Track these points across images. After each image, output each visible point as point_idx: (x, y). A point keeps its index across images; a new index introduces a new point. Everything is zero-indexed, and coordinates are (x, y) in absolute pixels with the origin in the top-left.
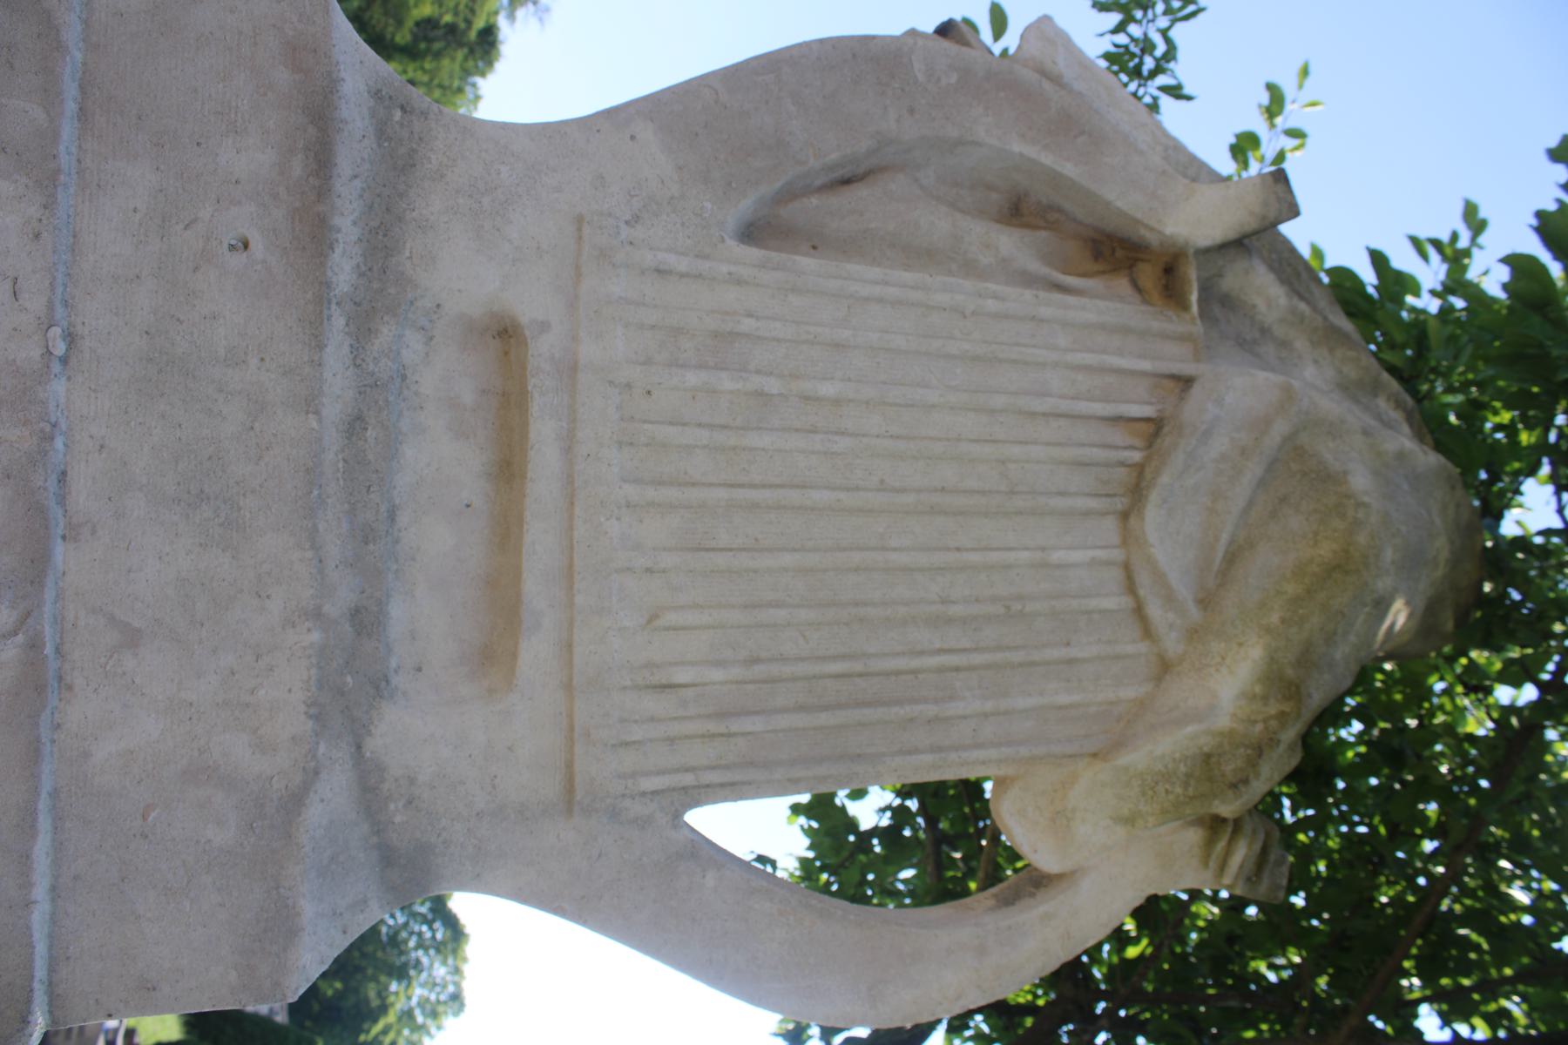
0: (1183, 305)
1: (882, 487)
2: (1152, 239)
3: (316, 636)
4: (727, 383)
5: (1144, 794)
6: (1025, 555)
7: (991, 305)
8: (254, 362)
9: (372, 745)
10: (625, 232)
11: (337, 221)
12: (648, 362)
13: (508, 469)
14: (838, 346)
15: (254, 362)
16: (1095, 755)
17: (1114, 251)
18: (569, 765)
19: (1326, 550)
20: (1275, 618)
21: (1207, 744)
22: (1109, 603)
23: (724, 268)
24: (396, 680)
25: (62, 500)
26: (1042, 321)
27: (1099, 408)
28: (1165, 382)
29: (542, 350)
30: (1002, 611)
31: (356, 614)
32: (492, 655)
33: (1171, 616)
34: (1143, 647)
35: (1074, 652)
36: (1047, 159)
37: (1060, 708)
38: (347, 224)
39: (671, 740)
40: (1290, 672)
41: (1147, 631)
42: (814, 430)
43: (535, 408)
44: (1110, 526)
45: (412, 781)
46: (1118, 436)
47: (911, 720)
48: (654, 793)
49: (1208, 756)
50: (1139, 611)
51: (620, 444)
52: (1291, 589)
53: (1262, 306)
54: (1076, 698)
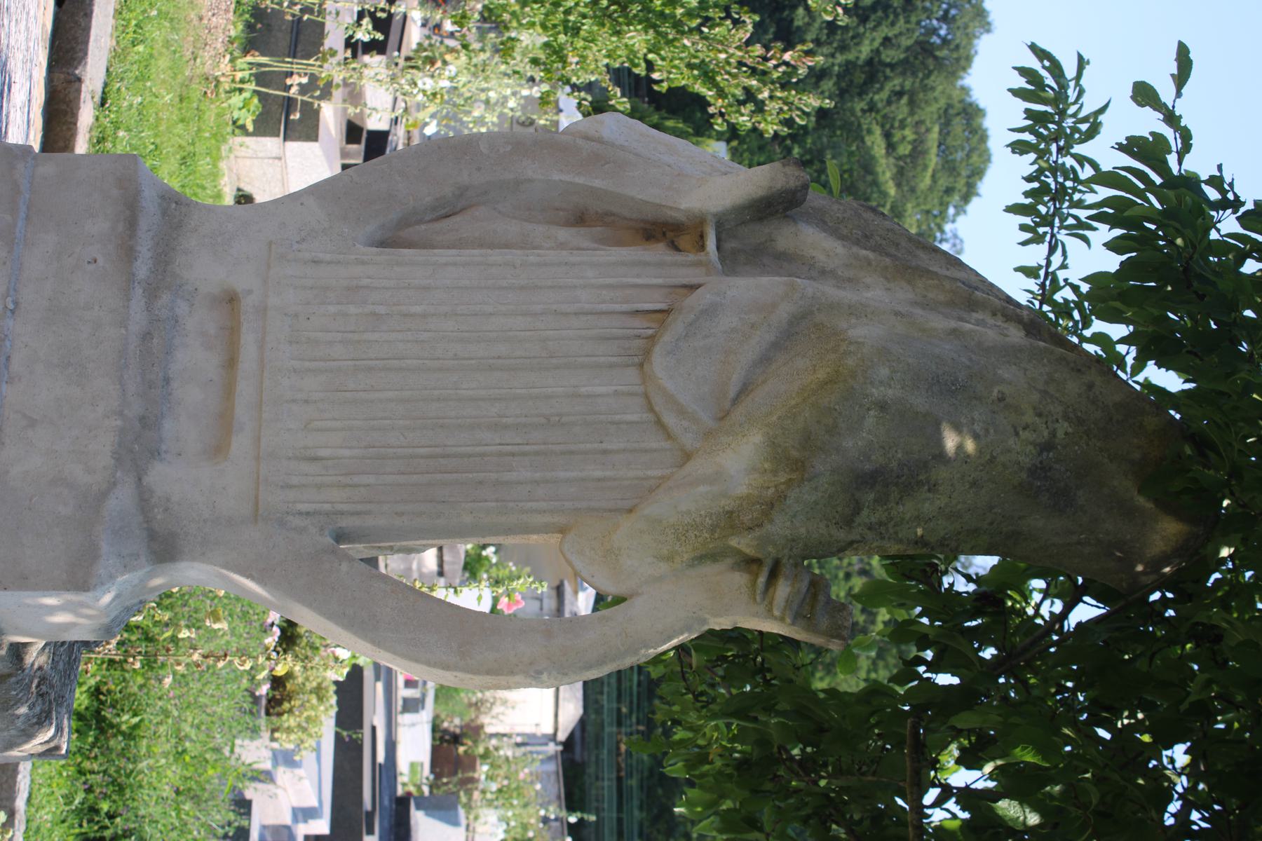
0: (702, 247)
1: (456, 357)
2: (681, 217)
3: (119, 423)
4: (352, 309)
5: (679, 540)
6: (561, 389)
7: (531, 258)
8: (97, 308)
9: (146, 480)
10: (296, 246)
11: (139, 248)
12: (308, 303)
13: (231, 363)
14: (427, 288)
15: (97, 308)
16: (630, 511)
17: (664, 234)
18: (257, 497)
19: (821, 375)
20: (774, 418)
21: (727, 504)
22: (635, 418)
23: (353, 257)
24: (163, 456)
25: (7, 367)
26: (574, 265)
27: (617, 307)
28: (678, 290)
29: (248, 303)
30: (543, 420)
31: (142, 419)
32: (218, 450)
33: (685, 423)
34: (666, 445)
35: (604, 446)
36: (580, 180)
37: (599, 480)
38: (145, 248)
39: (319, 487)
40: (795, 453)
41: (669, 436)
42: (409, 330)
43: (244, 329)
44: (632, 375)
45: (168, 500)
46: (637, 322)
47: (481, 483)
48: (308, 513)
49: (731, 513)
50: (659, 423)
51: (290, 342)
52: (793, 402)
53: (821, 257)
54: (608, 473)
